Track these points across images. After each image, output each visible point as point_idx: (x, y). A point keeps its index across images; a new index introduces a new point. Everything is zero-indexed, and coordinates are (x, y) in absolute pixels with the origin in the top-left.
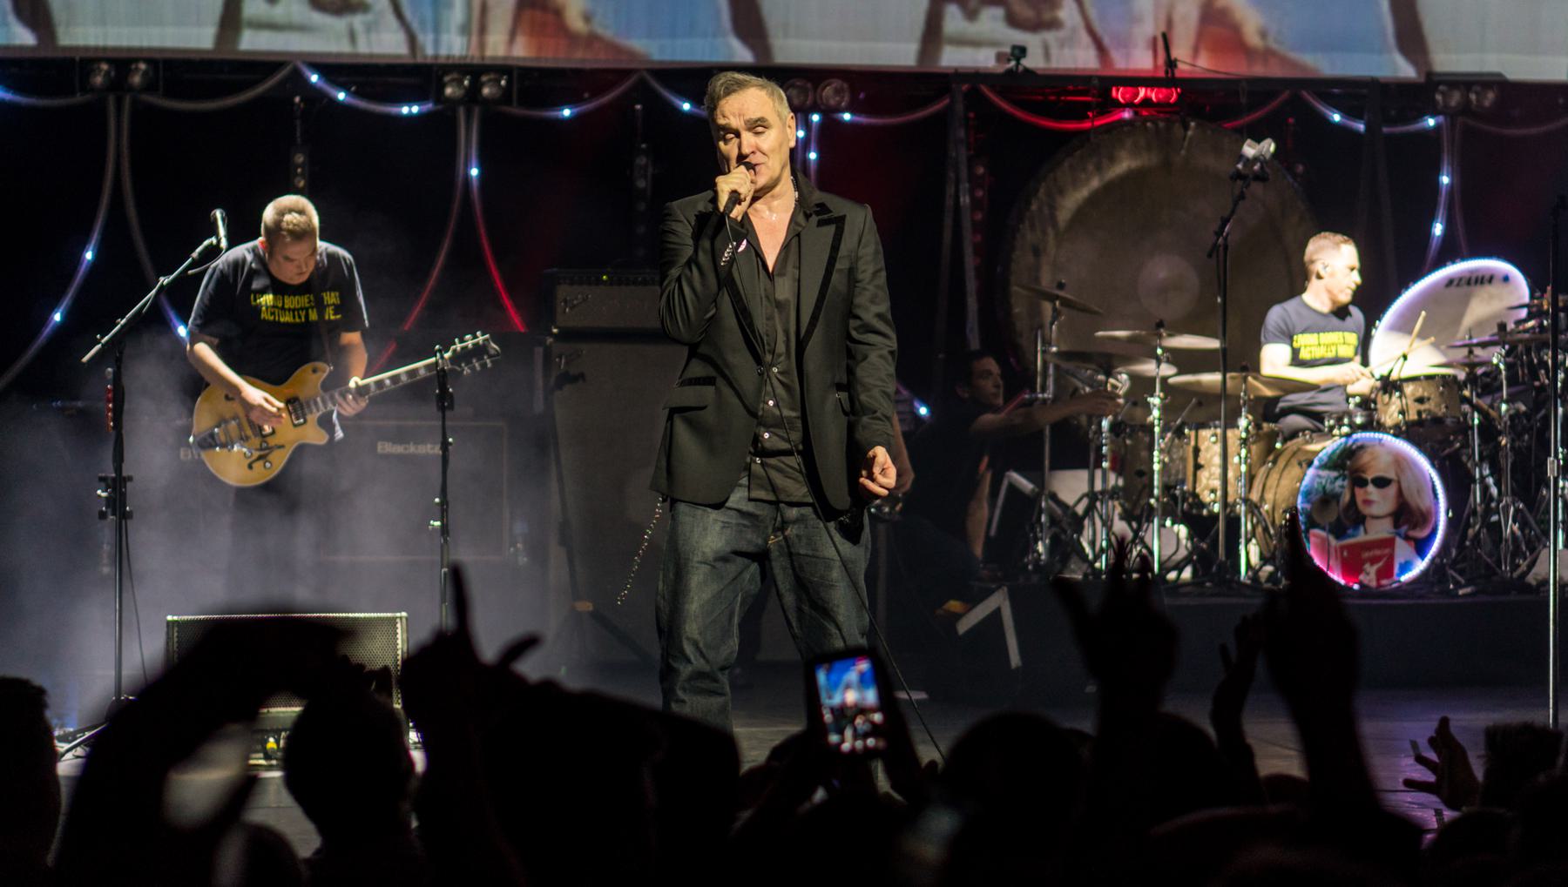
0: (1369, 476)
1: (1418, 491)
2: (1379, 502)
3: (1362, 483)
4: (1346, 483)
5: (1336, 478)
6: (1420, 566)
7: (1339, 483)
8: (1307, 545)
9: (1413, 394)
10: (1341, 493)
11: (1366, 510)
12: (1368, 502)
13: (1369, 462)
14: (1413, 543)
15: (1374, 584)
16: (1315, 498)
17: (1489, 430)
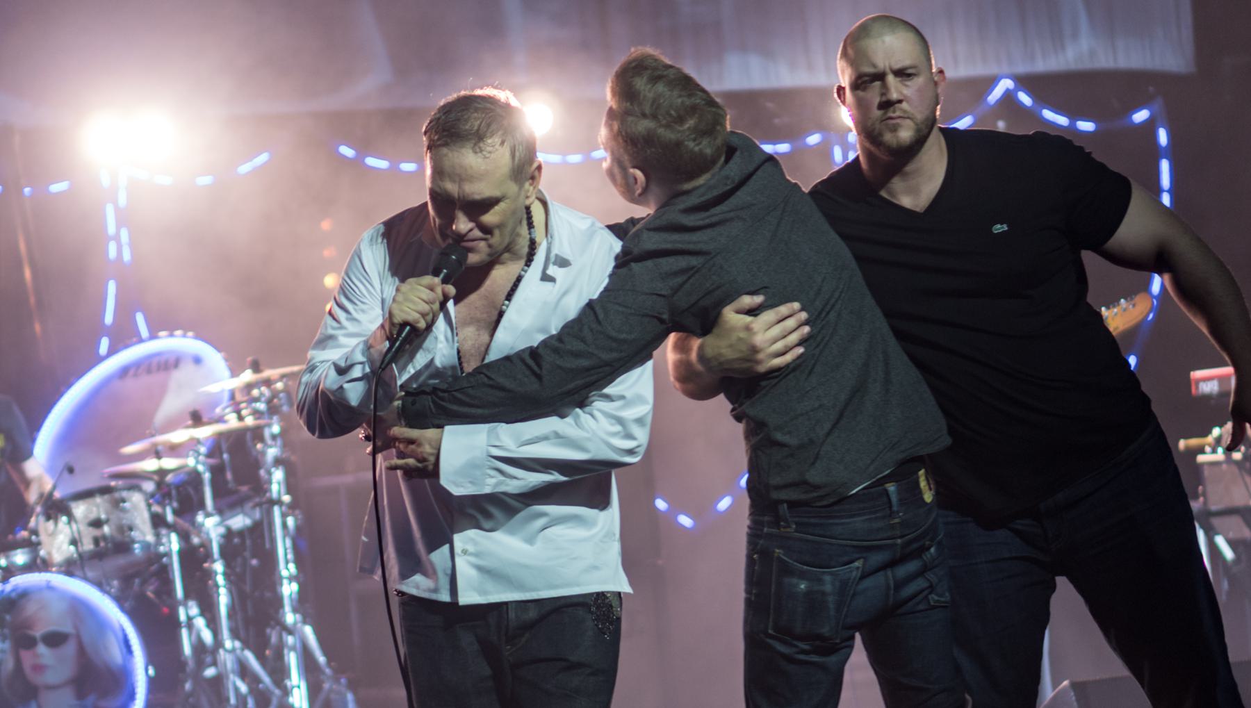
0: (38, 633)
9: (86, 517)
11: (38, 679)
12: (39, 668)
17: (194, 558)
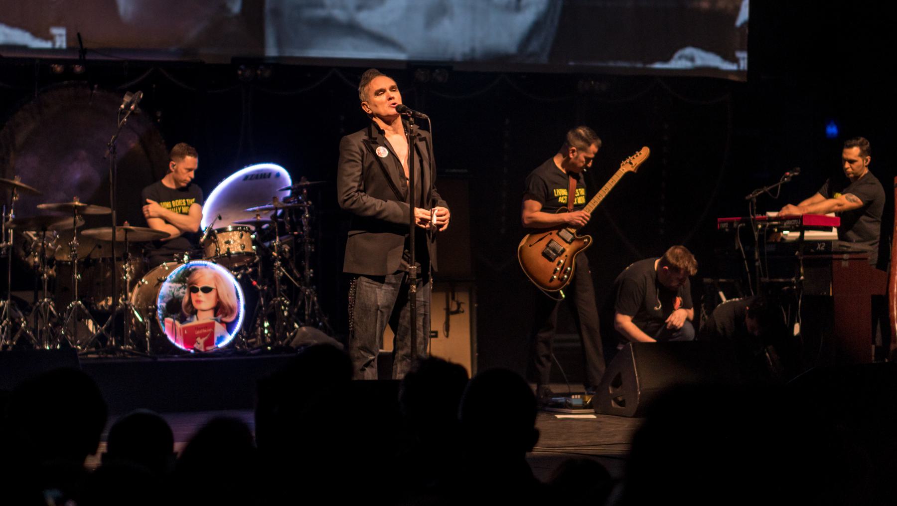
0: (199, 286)
1: (228, 295)
2: (205, 302)
3: (195, 290)
4: (186, 291)
5: (180, 288)
6: (229, 338)
7: (182, 290)
8: (163, 327)
10: (183, 296)
11: (197, 306)
12: (199, 302)
13: (199, 278)
14: (225, 325)
15: (202, 350)
16: (167, 300)
